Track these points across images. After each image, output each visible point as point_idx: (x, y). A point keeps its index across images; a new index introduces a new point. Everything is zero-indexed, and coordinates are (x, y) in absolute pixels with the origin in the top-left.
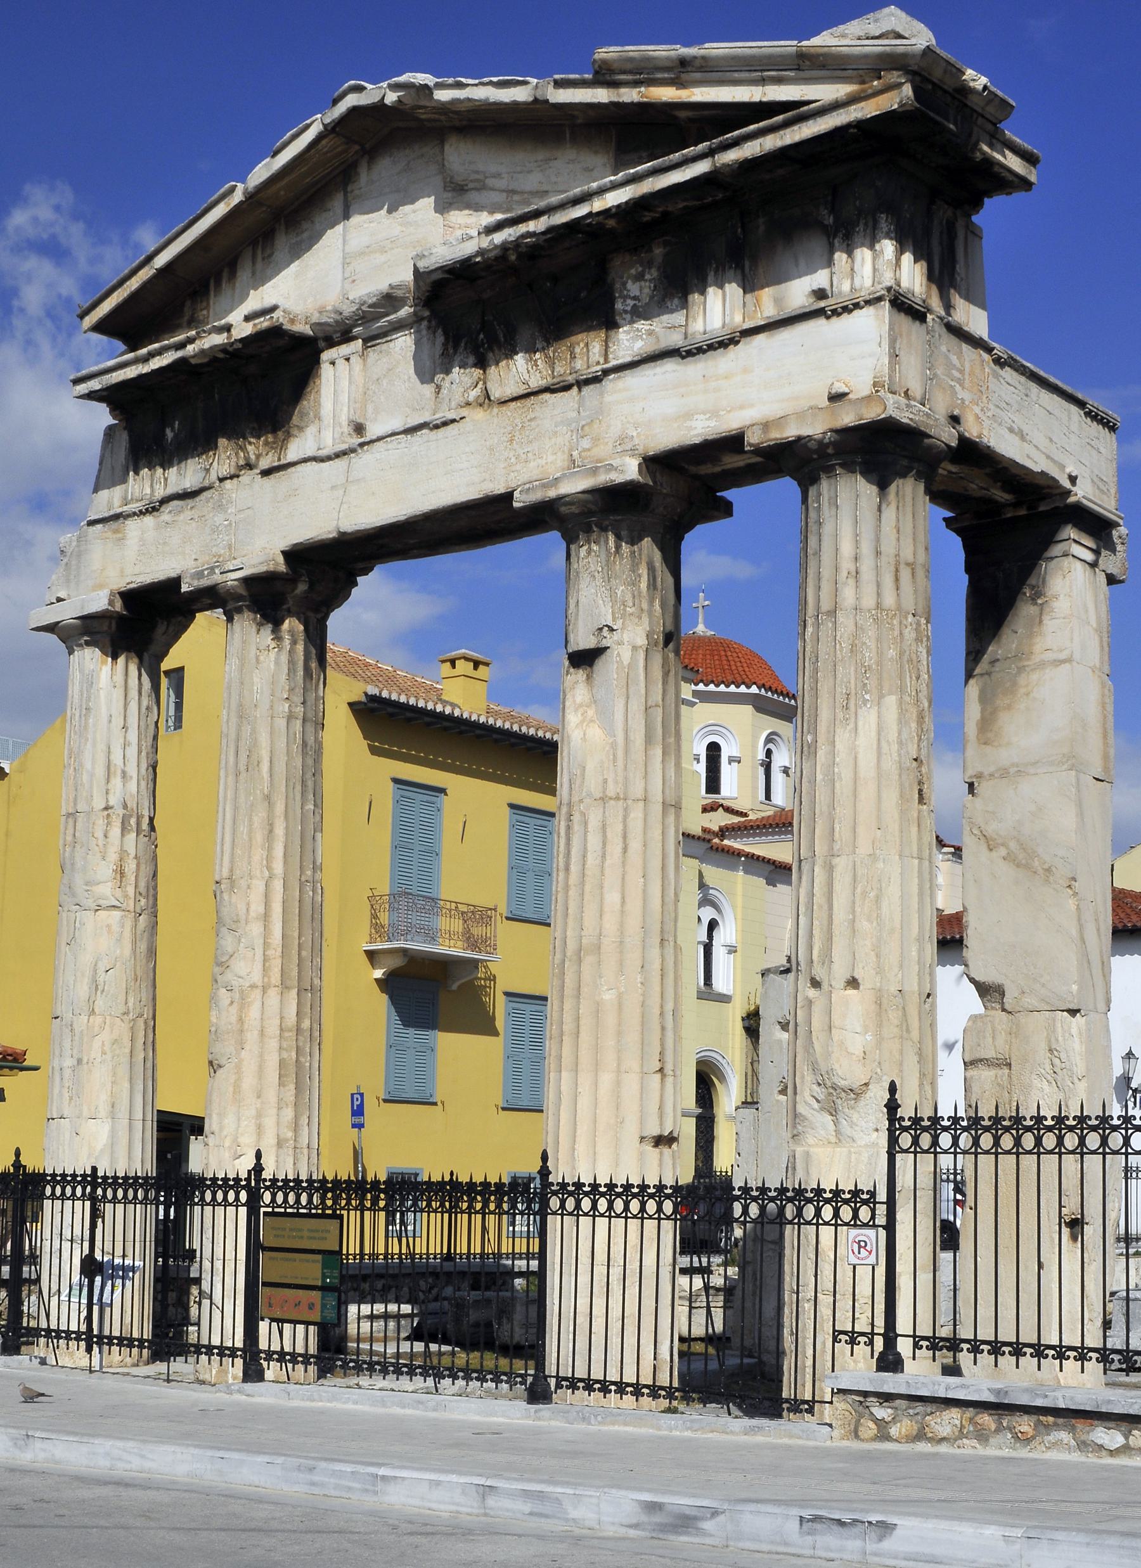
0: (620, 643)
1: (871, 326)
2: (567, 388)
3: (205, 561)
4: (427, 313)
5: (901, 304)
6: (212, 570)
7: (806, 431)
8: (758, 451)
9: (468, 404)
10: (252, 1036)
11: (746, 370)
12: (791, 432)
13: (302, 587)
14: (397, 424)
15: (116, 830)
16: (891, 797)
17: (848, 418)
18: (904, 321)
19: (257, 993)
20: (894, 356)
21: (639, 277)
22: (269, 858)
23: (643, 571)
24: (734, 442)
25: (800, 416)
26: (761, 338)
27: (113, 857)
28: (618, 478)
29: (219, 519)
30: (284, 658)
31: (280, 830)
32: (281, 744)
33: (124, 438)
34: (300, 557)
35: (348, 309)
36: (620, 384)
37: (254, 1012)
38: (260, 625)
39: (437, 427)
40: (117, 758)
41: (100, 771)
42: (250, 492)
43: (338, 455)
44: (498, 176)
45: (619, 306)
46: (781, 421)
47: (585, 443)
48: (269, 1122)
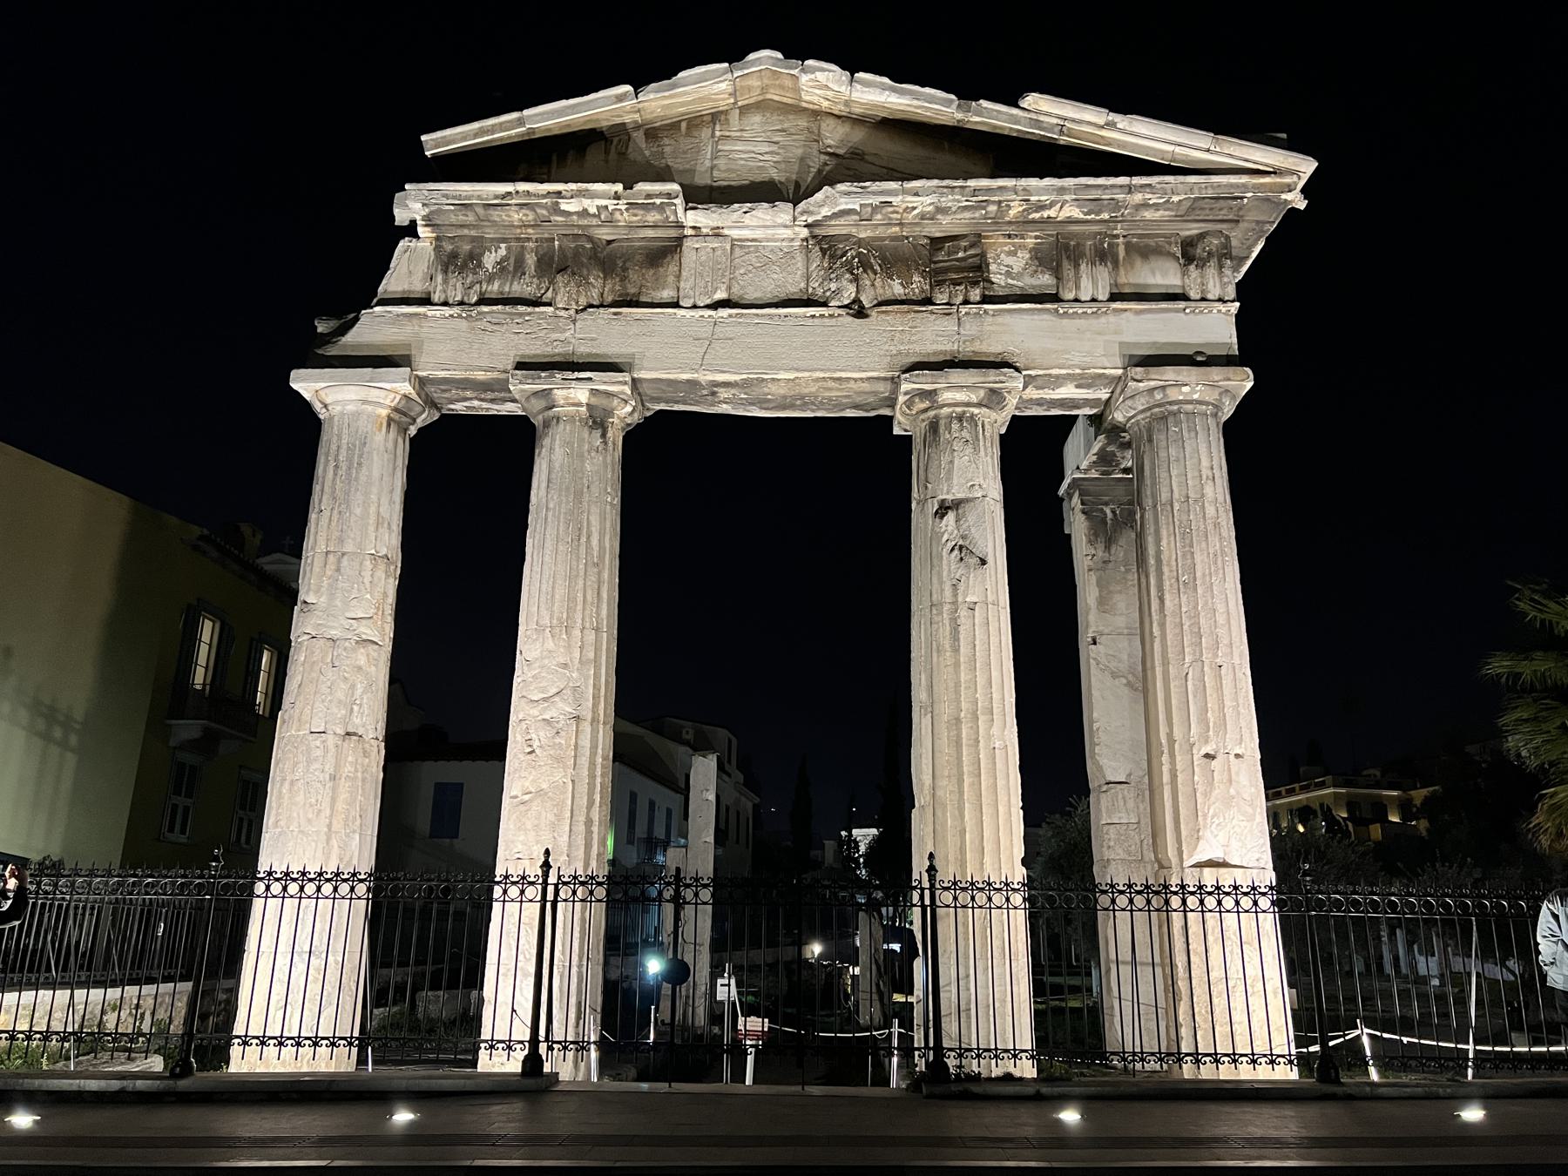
4: (805, 233)
21: (1013, 254)
41: (372, 520)
45: (993, 267)
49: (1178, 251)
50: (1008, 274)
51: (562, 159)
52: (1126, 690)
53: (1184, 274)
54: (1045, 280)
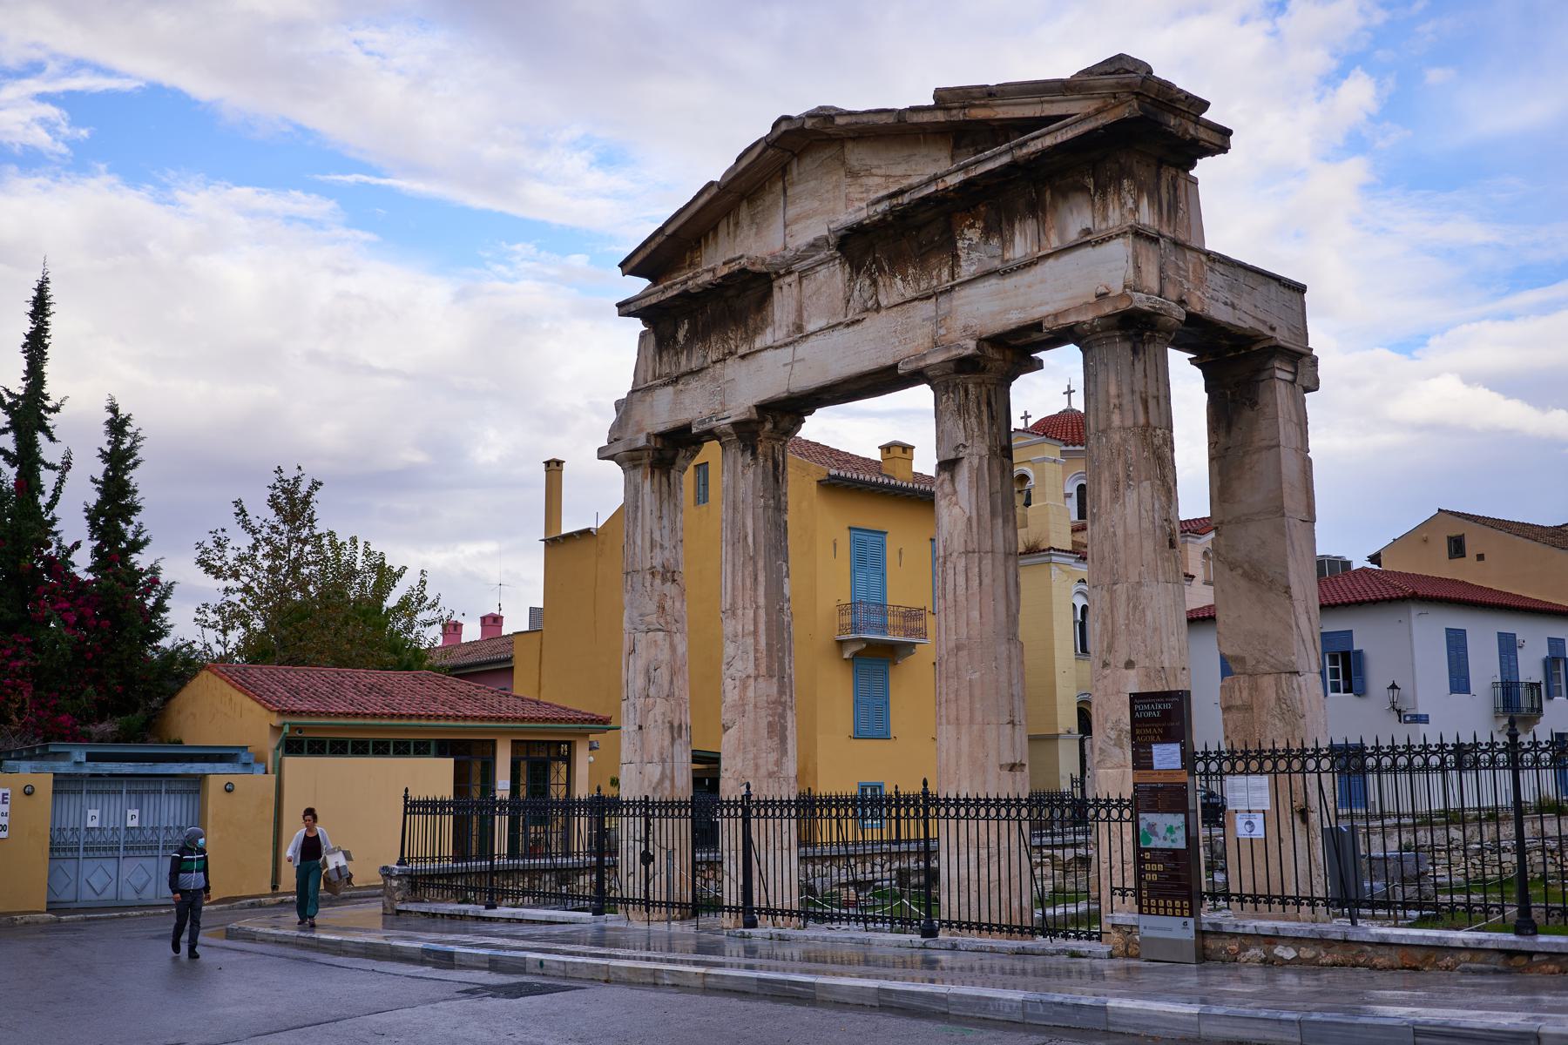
0: (971, 455)
1: (1120, 249)
2: (929, 298)
3: (706, 413)
5: (1138, 233)
6: (711, 419)
7: (1082, 318)
8: (1051, 332)
9: (867, 310)
10: (750, 707)
11: (1042, 282)
12: (1072, 319)
13: (769, 426)
14: (822, 323)
15: (658, 581)
16: (1149, 545)
17: (1108, 309)
18: (1142, 244)
19: (752, 681)
20: (1137, 268)
21: (972, 226)
22: (756, 596)
23: (984, 408)
24: (1037, 326)
25: (1077, 309)
26: (1051, 261)
27: (656, 598)
28: (966, 353)
29: (711, 387)
30: (760, 471)
31: (762, 578)
32: (761, 524)
33: (652, 339)
34: (764, 408)
35: (789, 254)
36: (963, 293)
37: (750, 693)
38: (743, 451)
39: (848, 325)
40: (657, 536)
42: (733, 368)
43: (786, 345)
44: (879, 167)
45: (960, 244)
46: (1066, 312)
47: (943, 331)
48: (761, 762)
49: (1090, 182)
51: (706, 237)
52: (1243, 584)
54: (995, 242)
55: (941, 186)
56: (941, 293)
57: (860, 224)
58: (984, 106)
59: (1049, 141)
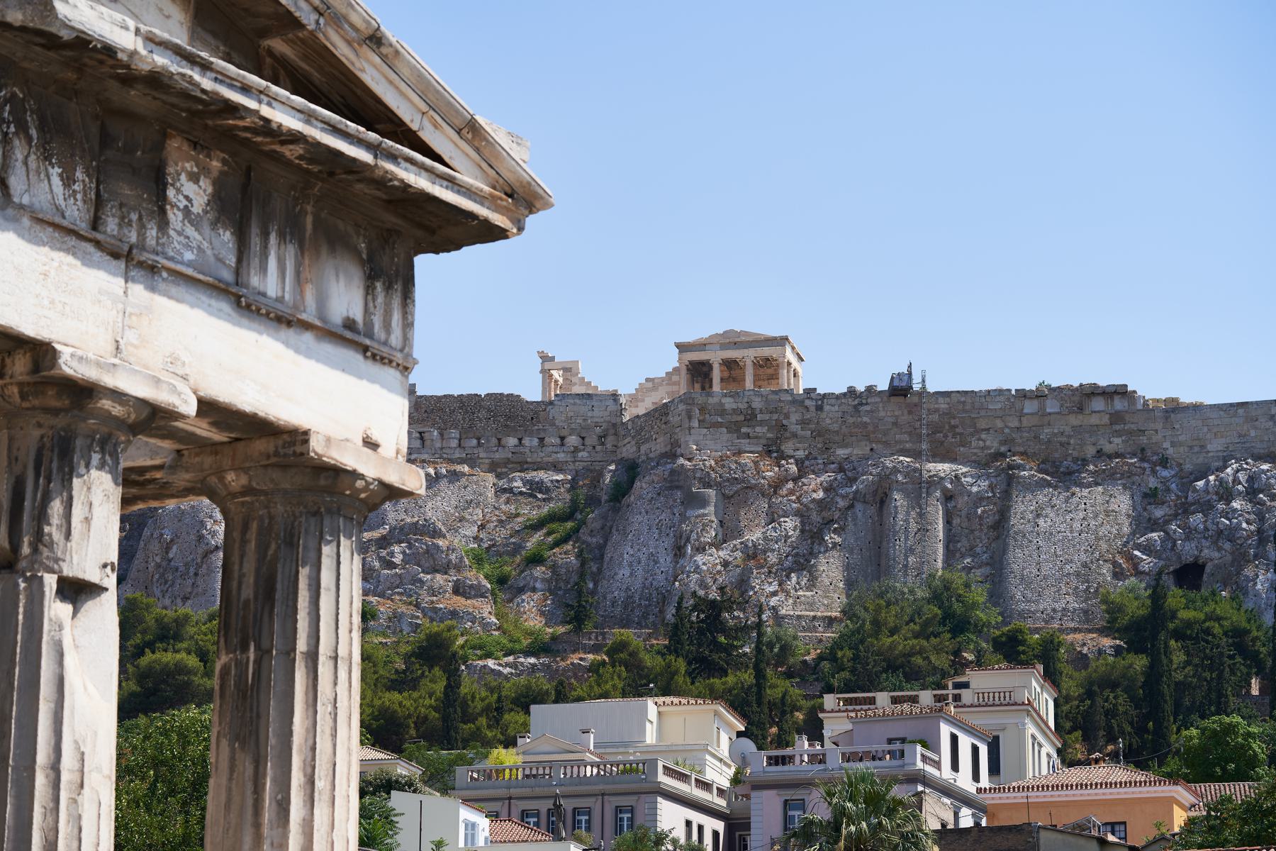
2: (115, 255)
7: (361, 469)
21: (194, 178)
45: (171, 193)
50: (187, 212)
53: (369, 290)
55: (266, 111)
56: (141, 264)
57: (109, 50)
58: (349, 43)
59: (420, 182)
